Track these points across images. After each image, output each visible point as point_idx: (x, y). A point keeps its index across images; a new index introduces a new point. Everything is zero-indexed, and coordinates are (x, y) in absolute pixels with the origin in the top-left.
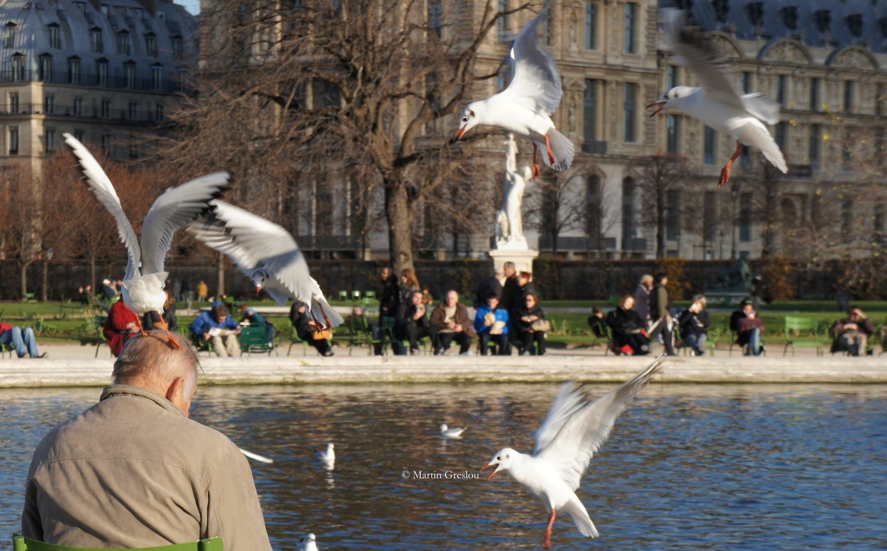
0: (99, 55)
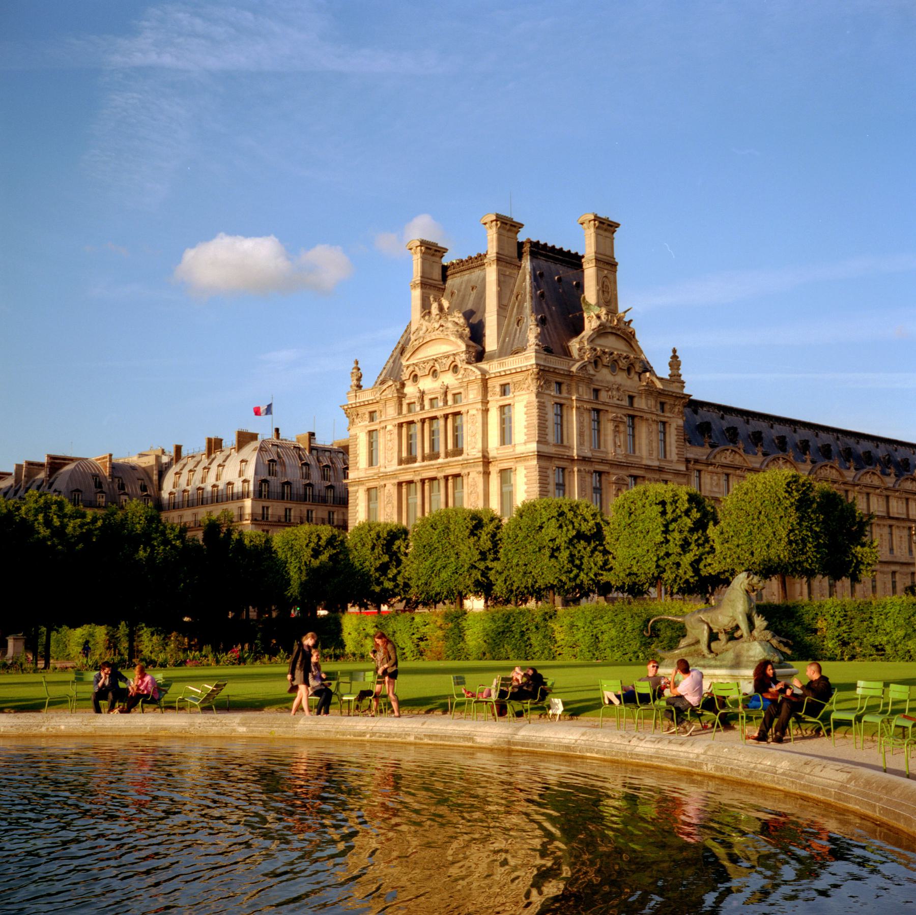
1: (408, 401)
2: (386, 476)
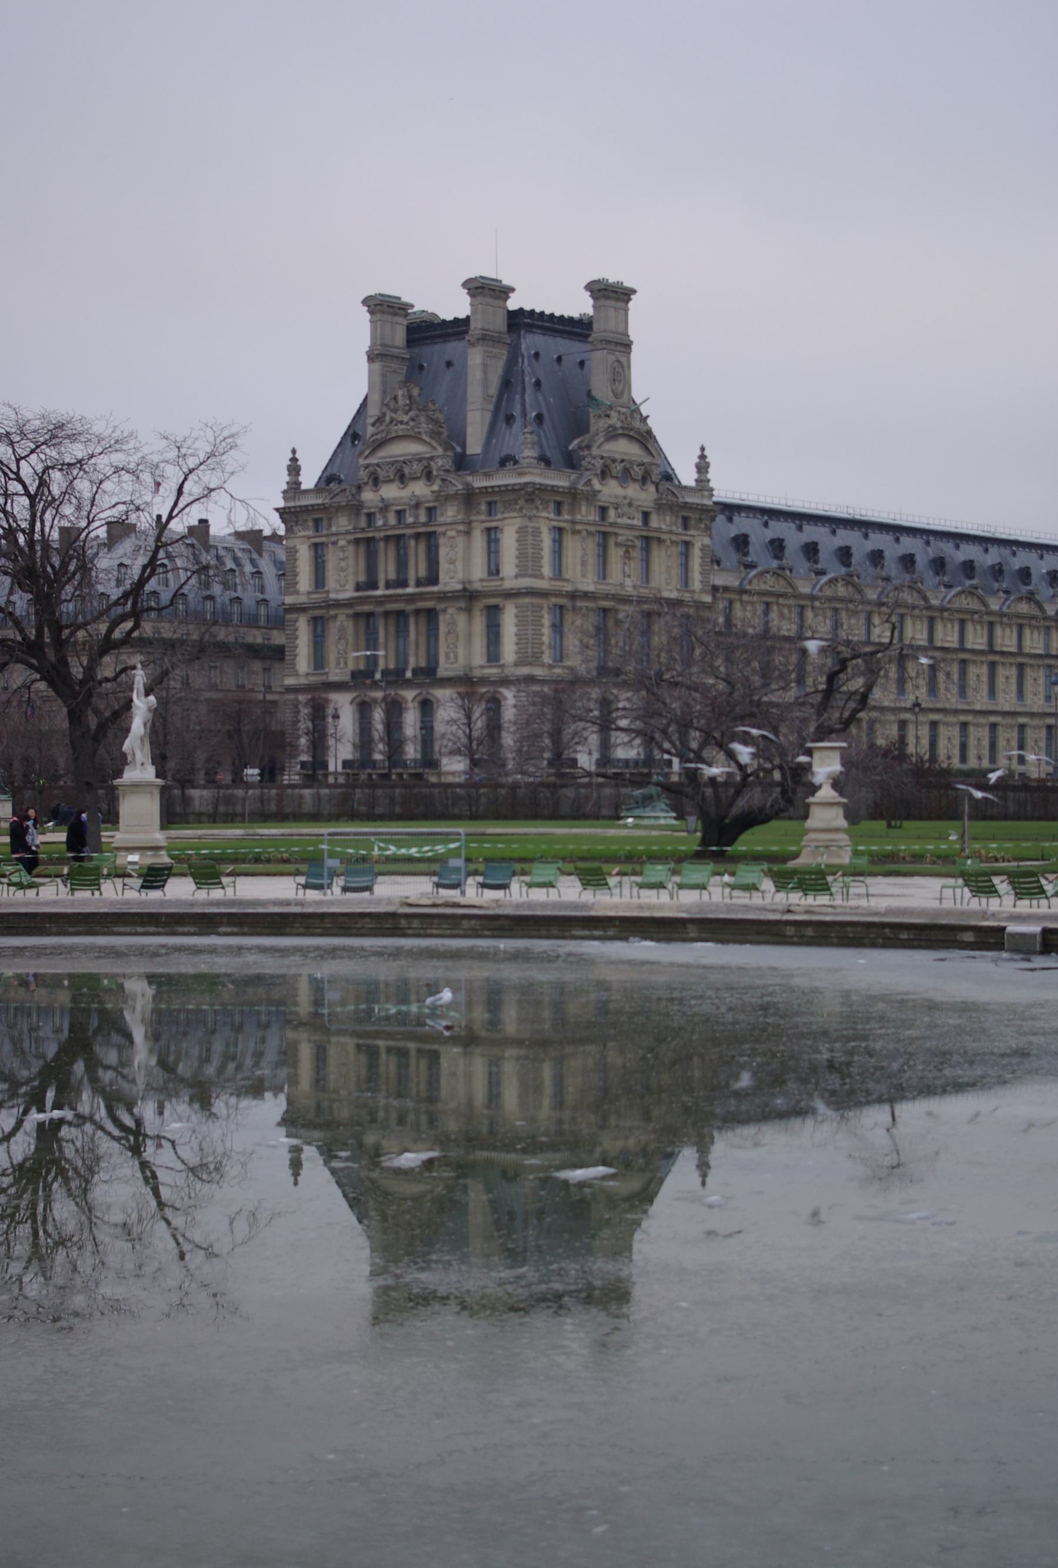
0: (205, 593)
1: (365, 511)
2: (338, 604)
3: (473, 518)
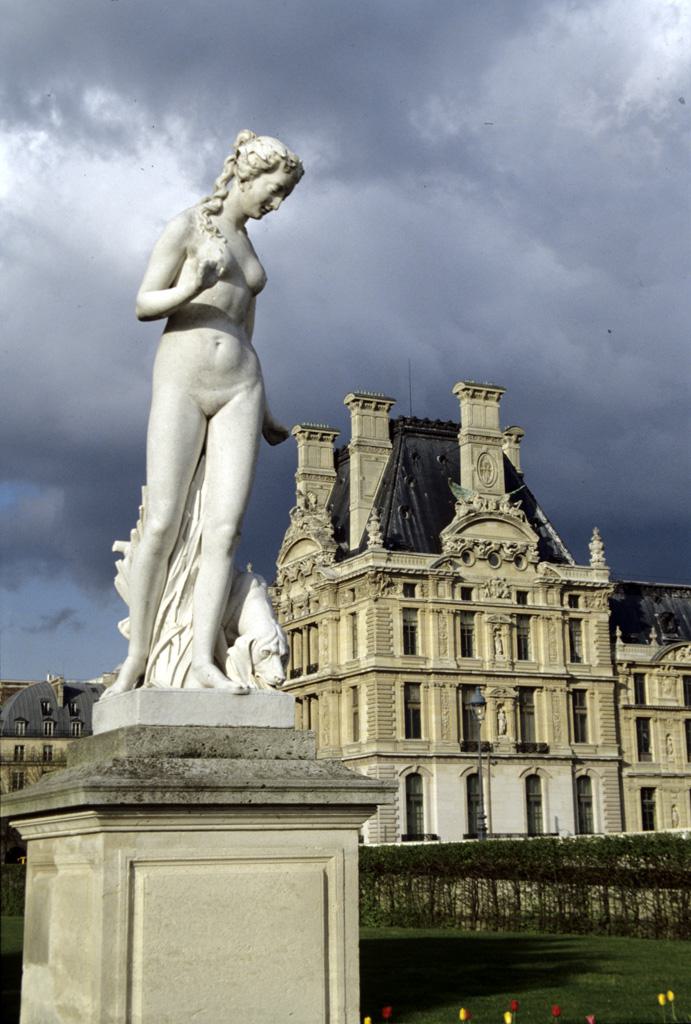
3: (341, 606)
